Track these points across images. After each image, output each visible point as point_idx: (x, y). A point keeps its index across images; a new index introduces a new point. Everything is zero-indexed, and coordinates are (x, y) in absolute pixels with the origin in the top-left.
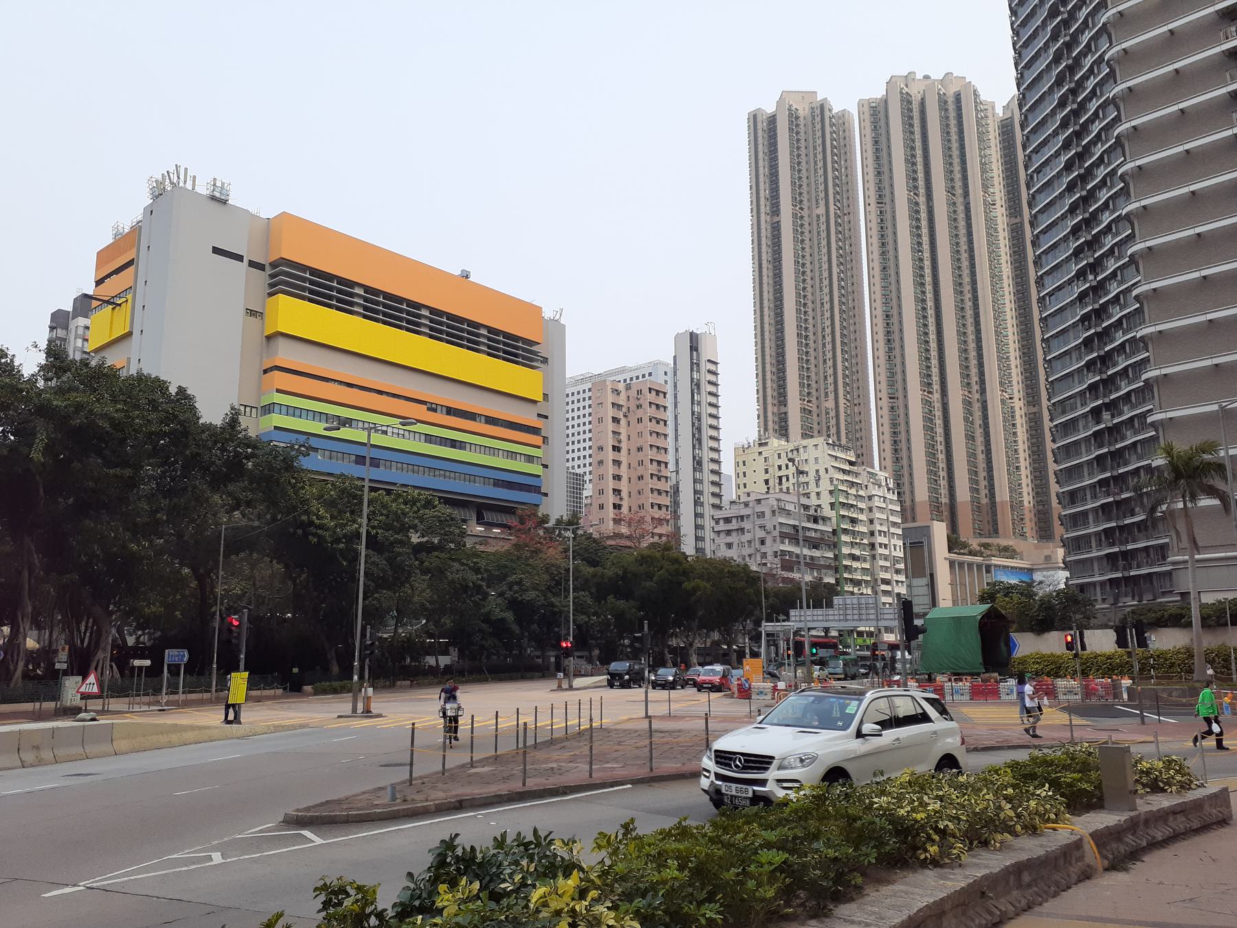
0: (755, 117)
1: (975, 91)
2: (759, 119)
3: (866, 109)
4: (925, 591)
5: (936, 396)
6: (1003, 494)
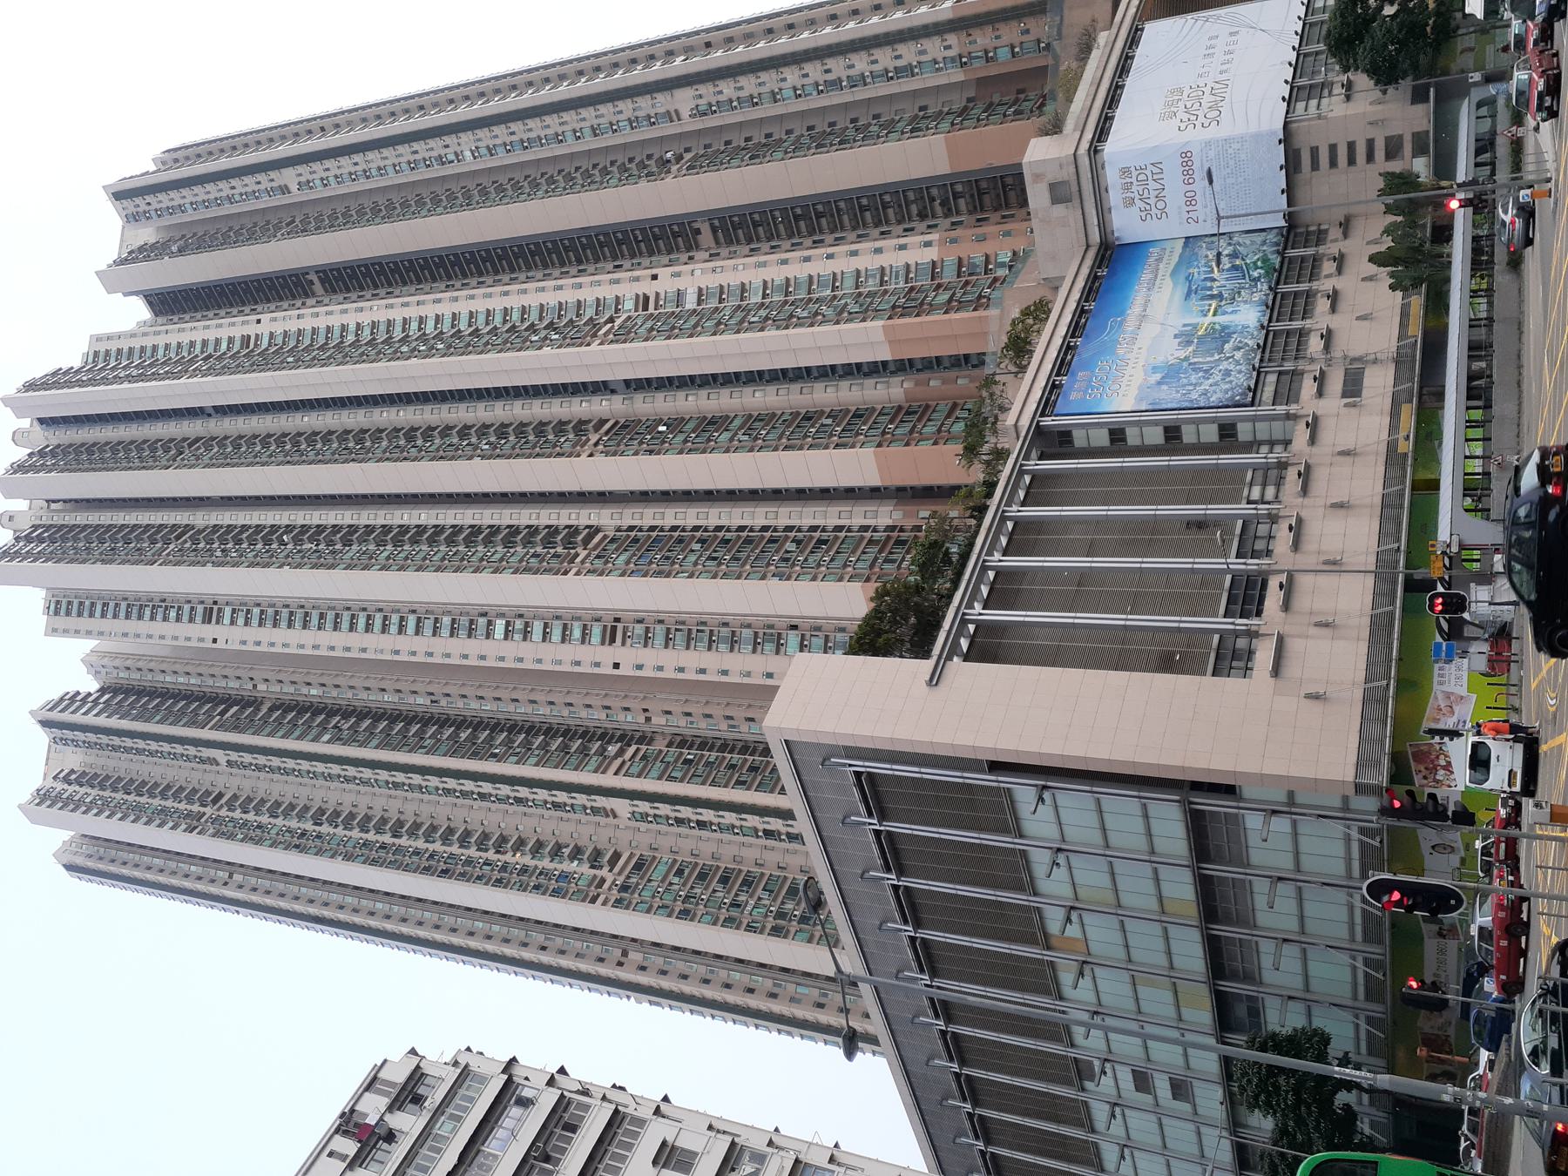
0: (70, 868)
1: (31, 386)
2: (80, 861)
3: (62, 622)
4: (1075, 803)
5: (606, 518)
6: (867, 339)
